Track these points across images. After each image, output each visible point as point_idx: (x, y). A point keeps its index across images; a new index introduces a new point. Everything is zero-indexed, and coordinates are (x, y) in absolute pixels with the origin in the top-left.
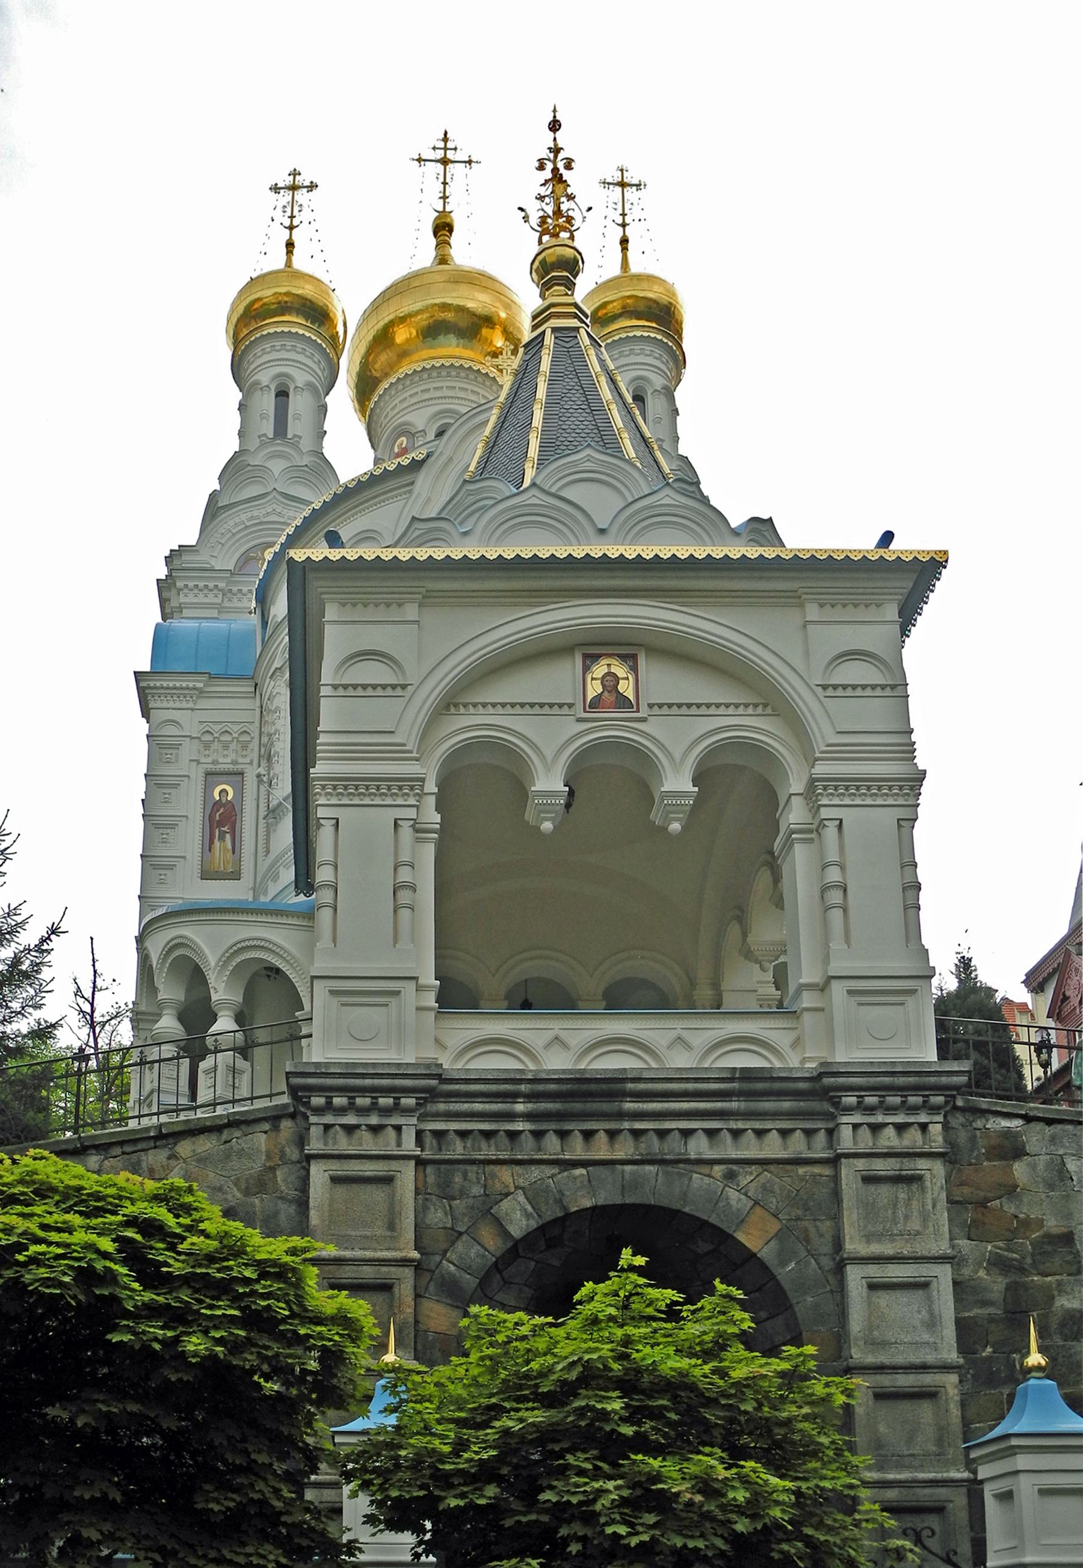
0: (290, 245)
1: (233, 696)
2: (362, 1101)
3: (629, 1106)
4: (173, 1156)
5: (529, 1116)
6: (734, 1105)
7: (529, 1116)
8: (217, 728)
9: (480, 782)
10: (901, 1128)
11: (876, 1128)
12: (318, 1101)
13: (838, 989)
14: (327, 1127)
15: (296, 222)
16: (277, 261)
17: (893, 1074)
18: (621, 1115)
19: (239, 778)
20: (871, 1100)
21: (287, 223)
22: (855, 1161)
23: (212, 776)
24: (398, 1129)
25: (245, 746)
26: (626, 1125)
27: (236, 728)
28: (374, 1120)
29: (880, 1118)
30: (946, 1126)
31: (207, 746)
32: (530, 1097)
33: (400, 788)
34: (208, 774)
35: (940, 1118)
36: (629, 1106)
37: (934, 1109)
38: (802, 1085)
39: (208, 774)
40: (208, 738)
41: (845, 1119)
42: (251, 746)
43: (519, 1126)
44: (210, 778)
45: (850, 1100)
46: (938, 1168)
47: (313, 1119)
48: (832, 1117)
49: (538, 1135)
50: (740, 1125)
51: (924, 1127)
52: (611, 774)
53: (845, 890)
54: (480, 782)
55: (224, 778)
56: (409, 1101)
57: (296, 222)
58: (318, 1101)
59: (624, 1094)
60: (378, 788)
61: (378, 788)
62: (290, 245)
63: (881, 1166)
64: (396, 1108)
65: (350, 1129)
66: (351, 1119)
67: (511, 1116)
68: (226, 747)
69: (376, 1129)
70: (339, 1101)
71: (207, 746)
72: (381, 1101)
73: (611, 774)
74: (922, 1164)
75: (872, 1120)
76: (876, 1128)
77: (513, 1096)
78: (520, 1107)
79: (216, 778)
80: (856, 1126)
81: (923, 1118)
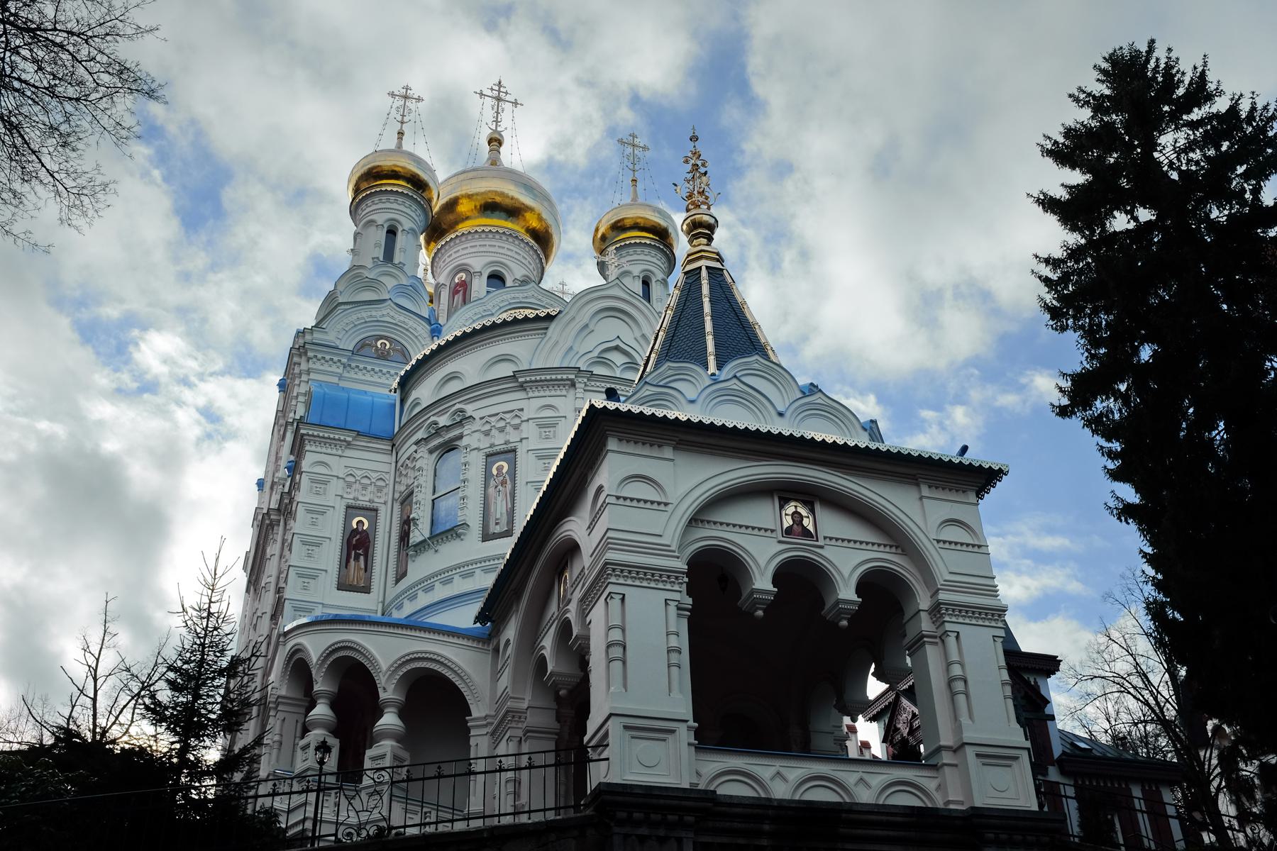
0: (401, 134)
1: (378, 451)
2: (655, 817)
8: (359, 473)
9: (712, 576)
12: (622, 815)
13: (970, 752)
14: (626, 836)
15: (406, 119)
16: (392, 145)
19: (373, 513)
20: (1003, 837)
21: (400, 118)
23: (351, 510)
24: (679, 840)
25: (380, 489)
27: (374, 475)
28: (662, 832)
31: (349, 485)
33: (669, 577)
34: (348, 507)
39: (348, 507)
40: (351, 479)
42: (385, 490)
43: (764, 842)
44: (350, 511)
47: (617, 830)
52: (802, 579)
53: (966, 682)
54: (712, 576)
55: (362, 512)
56: (690, 819)
57: (406, 119)
58: (622, 815)
60: (653, 575)
61: (653, 575)
62: (401, 134)
65: (642, 839)
66: (644, 831)
68: (365, 487)
70: (637, 815)
71: (349, 485)
72: (670, 817)
73: (802, 579)
78: (766, 827)
79: (354, 511)
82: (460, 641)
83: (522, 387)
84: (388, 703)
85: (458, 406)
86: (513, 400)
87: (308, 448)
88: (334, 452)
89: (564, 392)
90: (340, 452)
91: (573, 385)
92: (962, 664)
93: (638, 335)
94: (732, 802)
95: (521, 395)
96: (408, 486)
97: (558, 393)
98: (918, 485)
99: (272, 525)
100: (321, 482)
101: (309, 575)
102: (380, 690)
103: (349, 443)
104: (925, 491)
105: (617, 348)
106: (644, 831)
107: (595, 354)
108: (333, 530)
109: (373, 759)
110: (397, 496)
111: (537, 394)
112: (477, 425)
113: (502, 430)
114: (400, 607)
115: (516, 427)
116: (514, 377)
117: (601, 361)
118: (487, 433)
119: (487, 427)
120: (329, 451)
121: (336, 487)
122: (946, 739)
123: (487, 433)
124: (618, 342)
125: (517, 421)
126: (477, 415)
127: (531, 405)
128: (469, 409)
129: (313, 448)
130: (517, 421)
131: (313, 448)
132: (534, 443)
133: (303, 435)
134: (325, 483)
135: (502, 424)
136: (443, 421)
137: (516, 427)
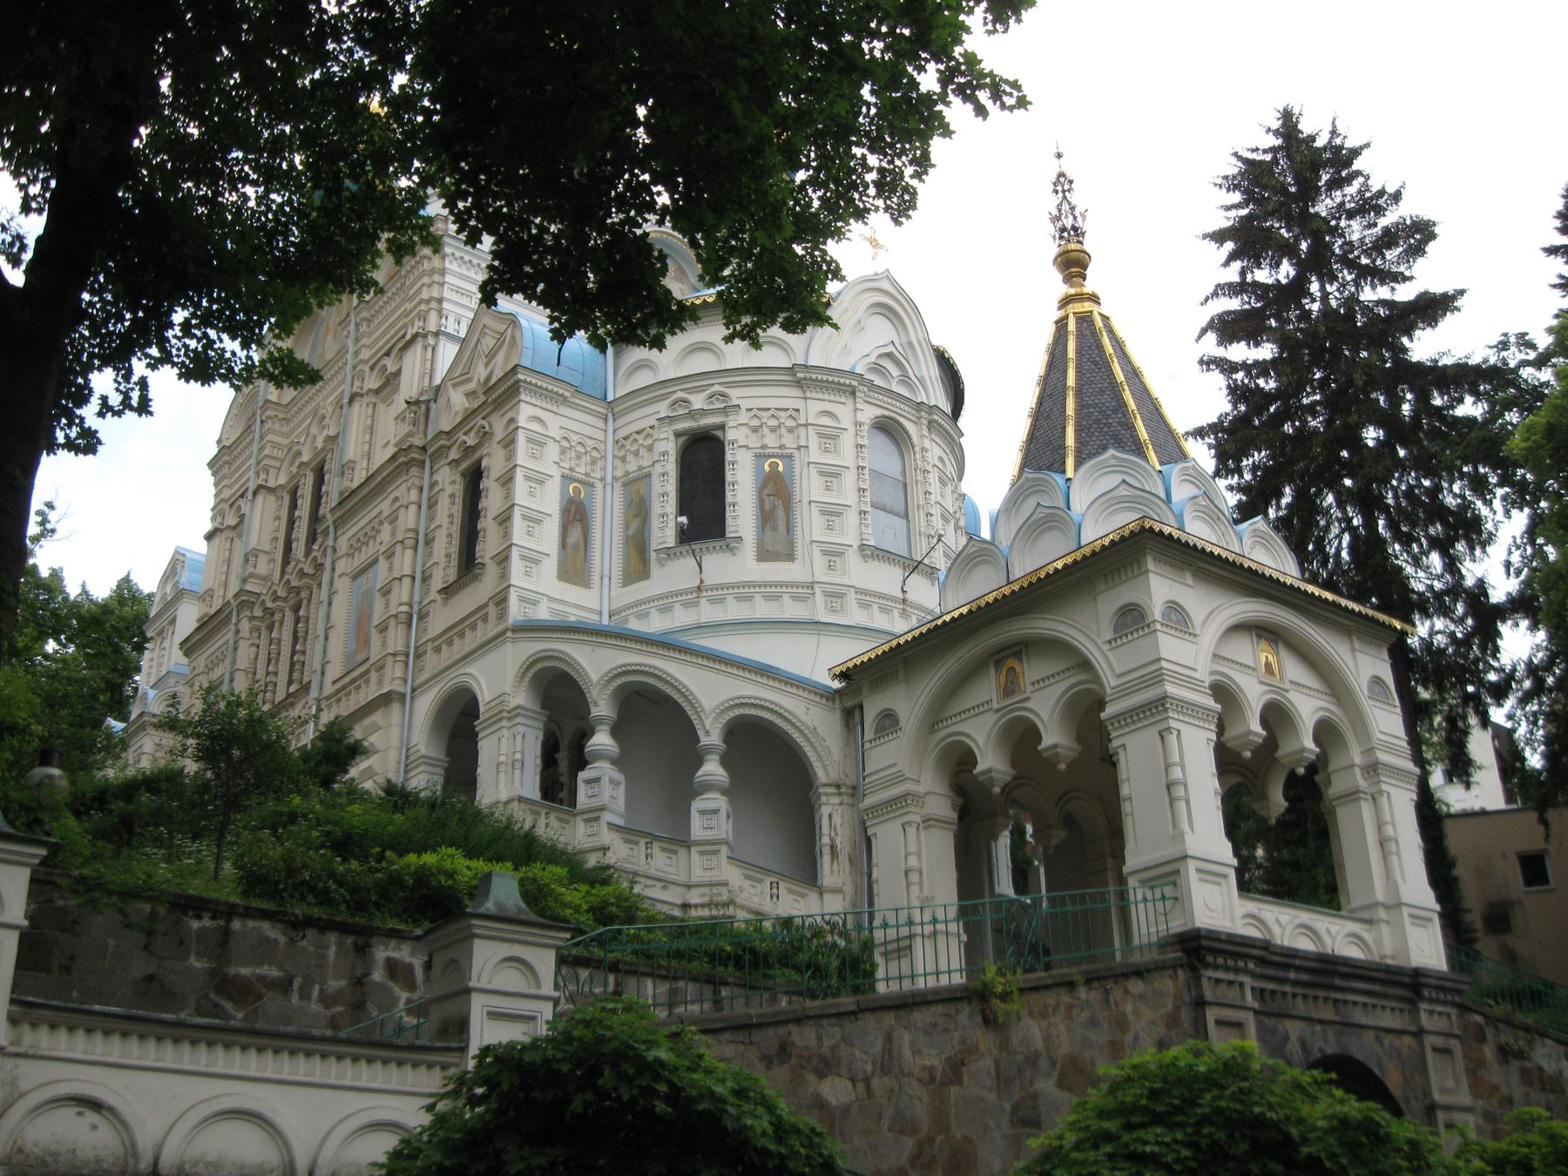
3: (1338, 982)
4: (1126, 992)
5: (1296, 983)
7: (1296, 983)
13: (1406, 911)
32: (1299, 969)
36: (1338, 982)
40: (565, 444)
43: (1287, 988)
49: (1294, 995)
59: (1334, 973)
64: (1246, 971)
68: (579, 457)
69: (1230, 983)
71: (563, 451)
82: (801, 693)
83: (798, 384)
84: (600, 720)
85: (717, 388)
86: (786, 397)
87: (523, 397)
88: (549, 407)
89: (843, 400)
90: (554, 408)
91: (853, 393)
92: (1394, 826)
93: (904, 341)
94: (1293, 953)
95: (796, 392)
96: (641, 468)
97: (838, 399)
98: (1350, 637)
99: (408, 465)
100: (537, 443)
101: (533, 559)
102: (701, 733)
103: (565, 399)
104: (1357, 645)
105: (889, 355)
107: (872, 359)
108: (550, 501)
109: (703, 812)
110: (619, 473)
111: (814, 395)
112: (743, 417)
113: (773, 430)
114: (644, 615)
115: (790, 430)
116: (792, 370)
117: (877, 369)
118: (755, 430)
119: (755, 422)
120: (544, 404)
121: (552, 451)
122: (1380, 896)
123: (755, 430)
124: (890, 349)
125: (791, 423)
126: (745, 404)
127: (814, 408)
128: (735, 394)
129: (528, 399)
130: (791, 423)
131: (528, 399)
132: (815, 455)
133: (518, 381)
134: (542, 444)
135: (773, 423)
136: (698, 401)
137: (790, 430)
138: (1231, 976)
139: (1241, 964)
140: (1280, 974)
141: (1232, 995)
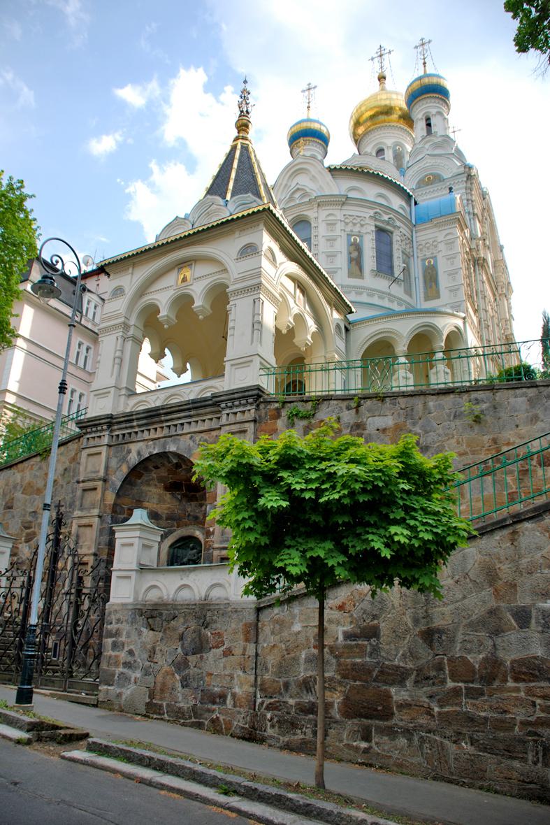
3: (163, 418)
5: (139, 426)
6: (192, 413)
7: (139, 426)
10: (243, 412)
11: (235, 413)
17: (234, 393)
18: (162, 422)
20: (229, 404)
22: (225, 427)
26: (165, 424)
28: (98, 434)
29: (235, 410)
30: (258, 408)
32: (138, 419)
35: (254, 407)
37: (251, 404)
38: (210, 402)
41: (224, 412)
43: (136, 430)
45: (223, 405)
46: (252, 425)
48: (220, 412)
49: (143, 431)
50: (196, 419)
51: (249, 410)
56: (105, 427)
63: (234, 428)
64: (102, 430)
66: (93, 435)
67: (132, 427)
74: (247, 425)
75: (232, 411)
76: (235, 413)
77: (132, 421)
80: (228, 414)
81: (248, 408)
106: (93, 435)
138: (98, 434)
139: (99, 428)
140: (128, 425)
141: (97, 442)
